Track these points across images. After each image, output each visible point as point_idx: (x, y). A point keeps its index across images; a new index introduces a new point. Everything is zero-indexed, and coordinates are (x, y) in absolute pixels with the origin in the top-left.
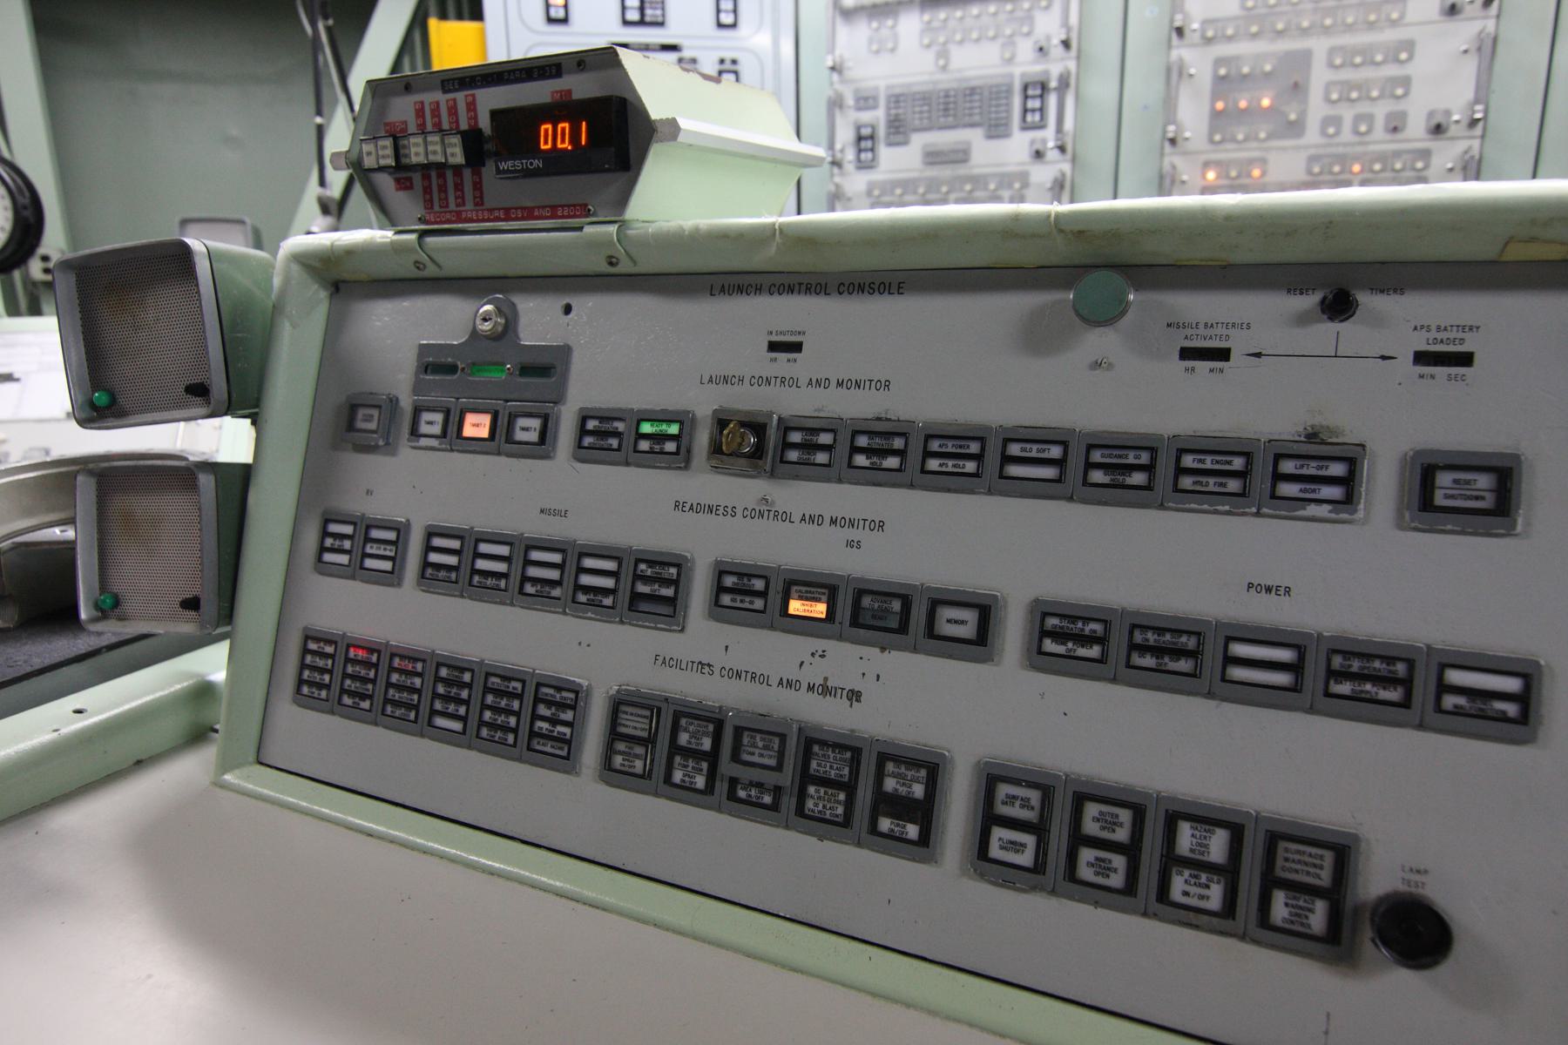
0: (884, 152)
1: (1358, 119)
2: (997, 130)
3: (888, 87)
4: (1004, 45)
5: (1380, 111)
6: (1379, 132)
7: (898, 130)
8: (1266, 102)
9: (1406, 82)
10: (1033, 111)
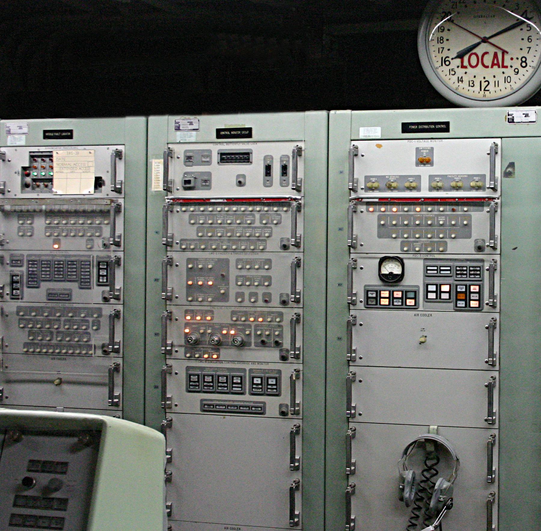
0: (27, 291)
1: (251, 295)
2: (85, 285)
3: (28, 256)
4: (87, 240)
5: (261, 291)
6: (260, 302)
7: (34, 281)
8: (210, 283)
9: (269, 279)
10: (103, 276)
